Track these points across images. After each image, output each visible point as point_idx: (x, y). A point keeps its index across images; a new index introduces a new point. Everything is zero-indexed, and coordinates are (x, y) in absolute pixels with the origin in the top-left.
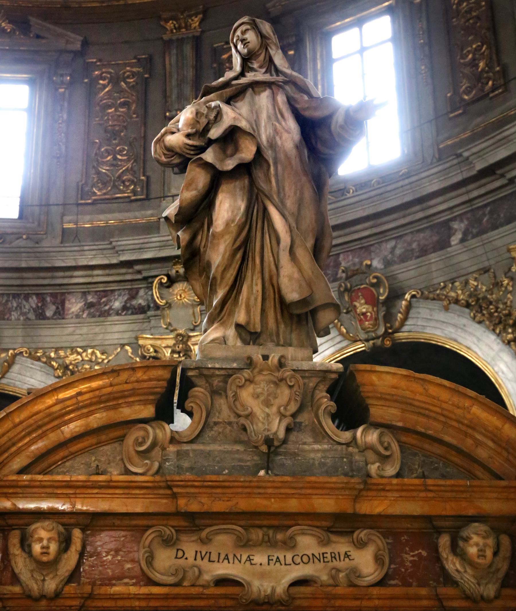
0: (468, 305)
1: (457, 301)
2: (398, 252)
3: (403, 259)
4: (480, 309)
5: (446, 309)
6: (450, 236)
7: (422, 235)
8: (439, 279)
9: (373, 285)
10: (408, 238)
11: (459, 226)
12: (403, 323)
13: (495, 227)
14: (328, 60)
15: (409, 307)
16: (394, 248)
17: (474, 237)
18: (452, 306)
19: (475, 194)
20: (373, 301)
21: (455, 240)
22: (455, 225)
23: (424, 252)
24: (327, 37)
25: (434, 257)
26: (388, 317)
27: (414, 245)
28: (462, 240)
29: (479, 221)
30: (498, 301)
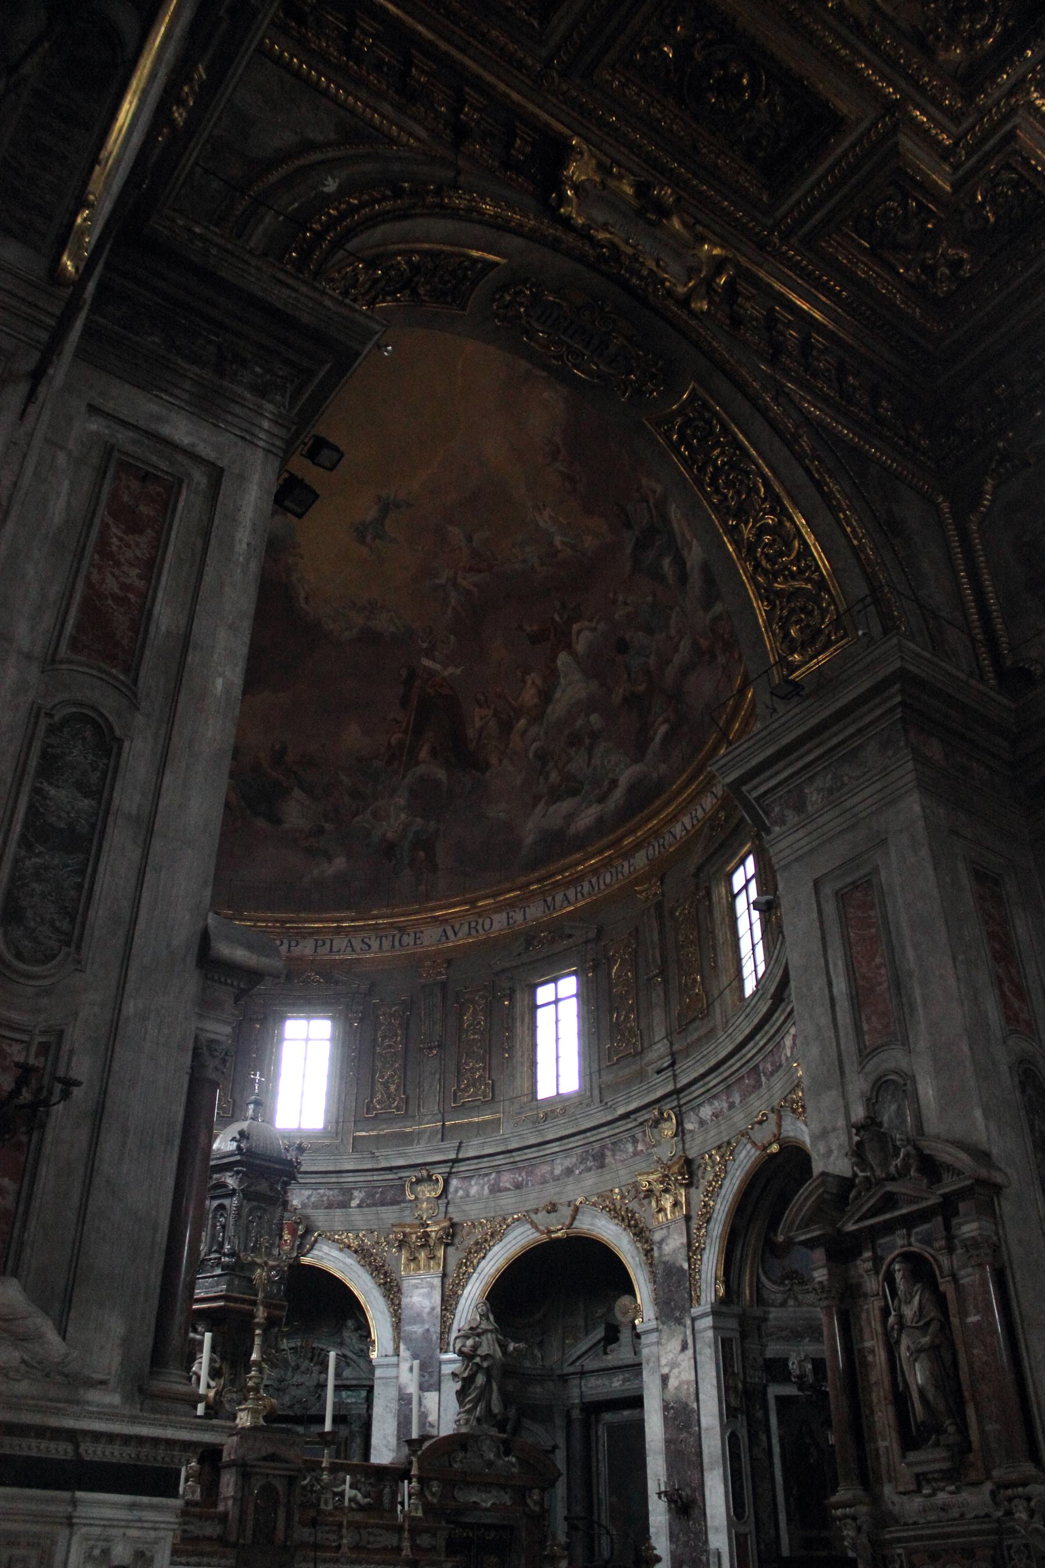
0: (356, 1252)
1: (349, 1247)
2: (313, 1199)
3: (315, 1206)
4: (364, 1257)
5: (341, 1250)
6: (351, 1199)
7: (331, 1193)
8: (337, 1226)
9: (296, 1223)
10: (321, 1191)
11: (358, 1196)
12: (308, 1252)
13: (383, 1205)
14: (281, 1039)
15: (316, 1241)
16: (309, 1197)
17: (368, 1206)
18: (346, 1250)
19: (375, 1178)
20: (293, 1232)
21: (354, 1203)
22: (356, 1193)
23: (330, 1206)
24: (283, 1018)
25: (338, 1212)
26: (301, 1246)
27: (325, 1198)
28: (359, 1206)
29: (373, 1196)
30: (377, 1255)
